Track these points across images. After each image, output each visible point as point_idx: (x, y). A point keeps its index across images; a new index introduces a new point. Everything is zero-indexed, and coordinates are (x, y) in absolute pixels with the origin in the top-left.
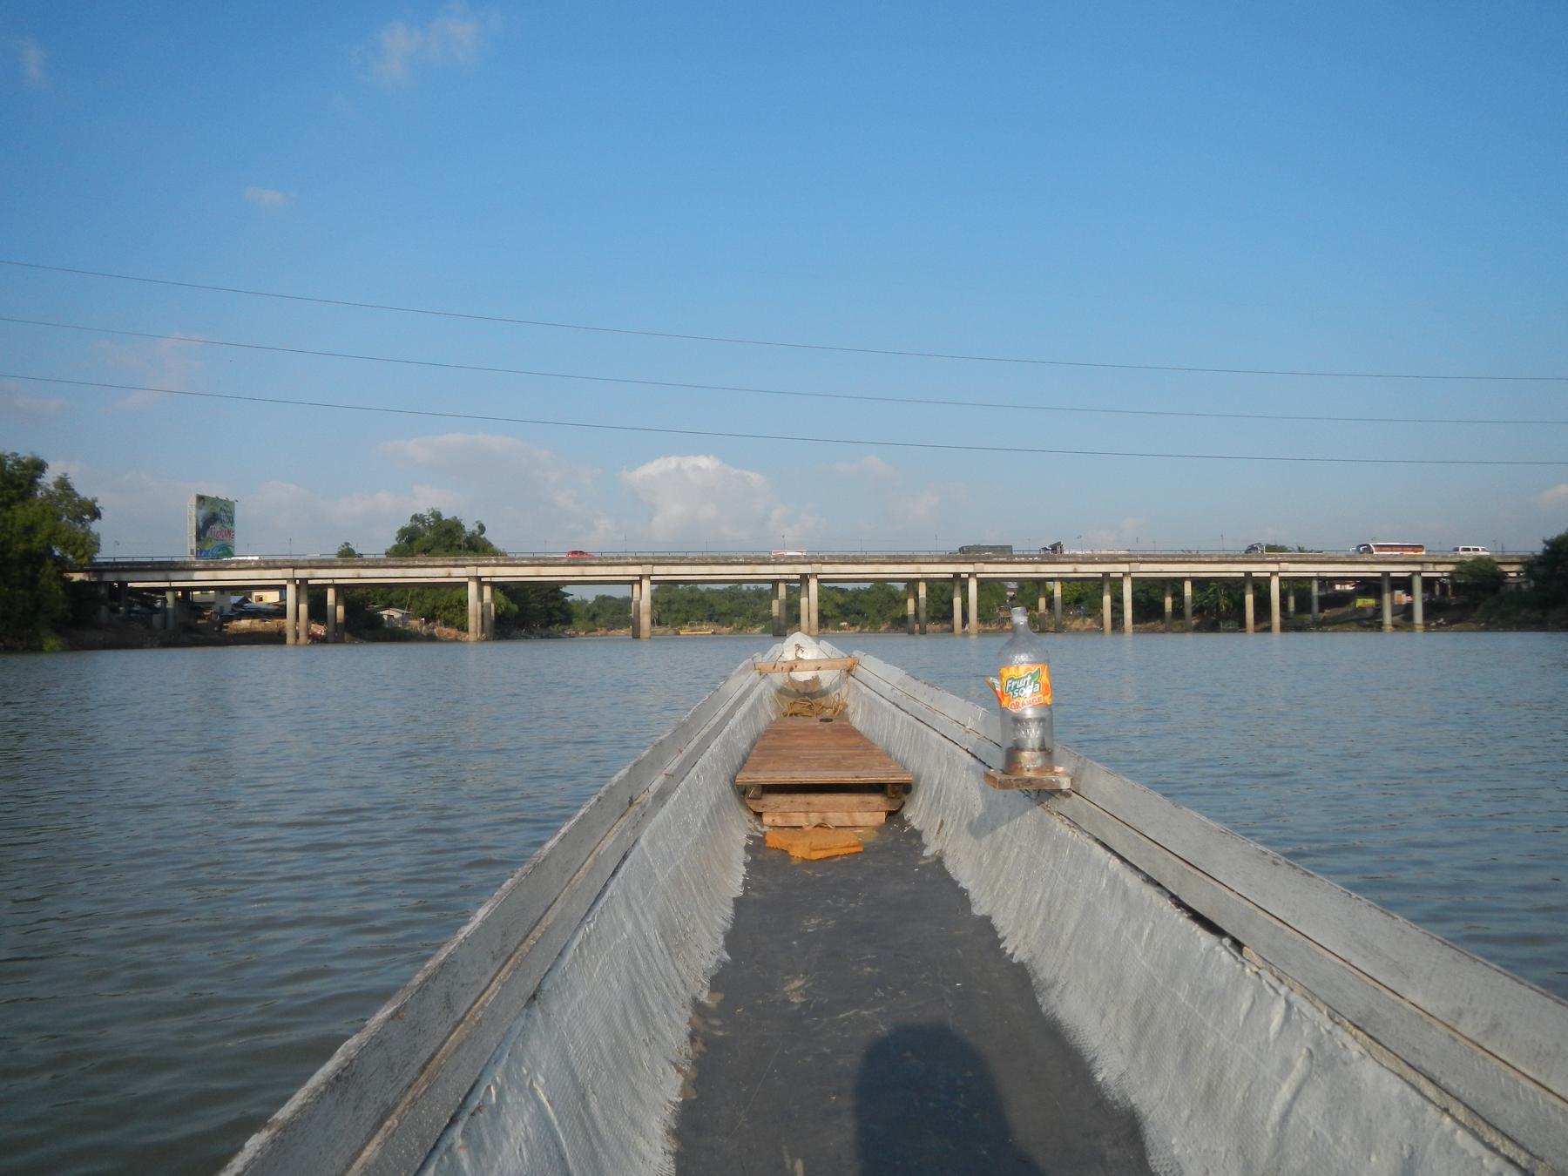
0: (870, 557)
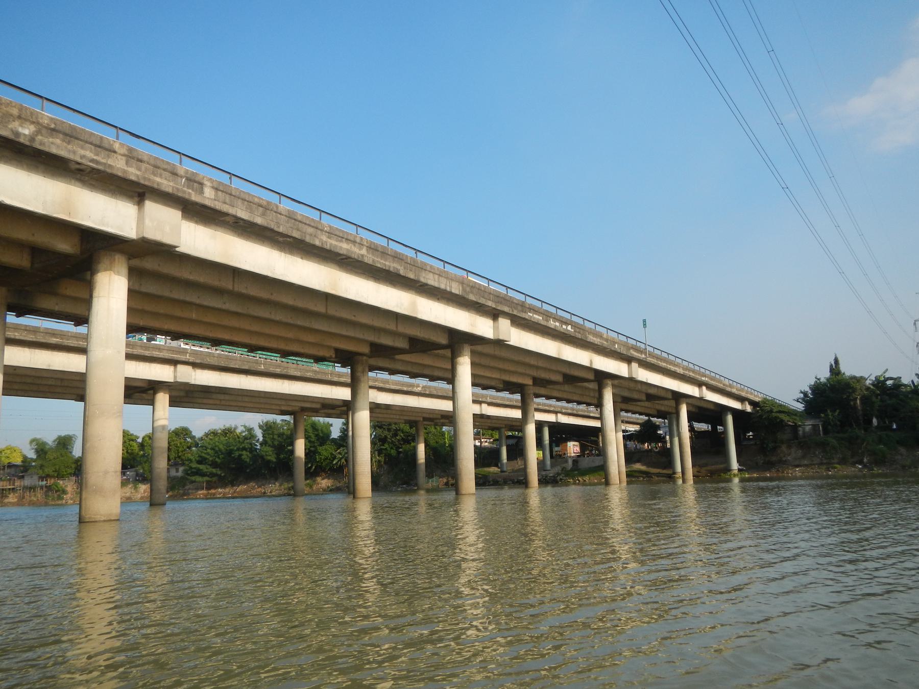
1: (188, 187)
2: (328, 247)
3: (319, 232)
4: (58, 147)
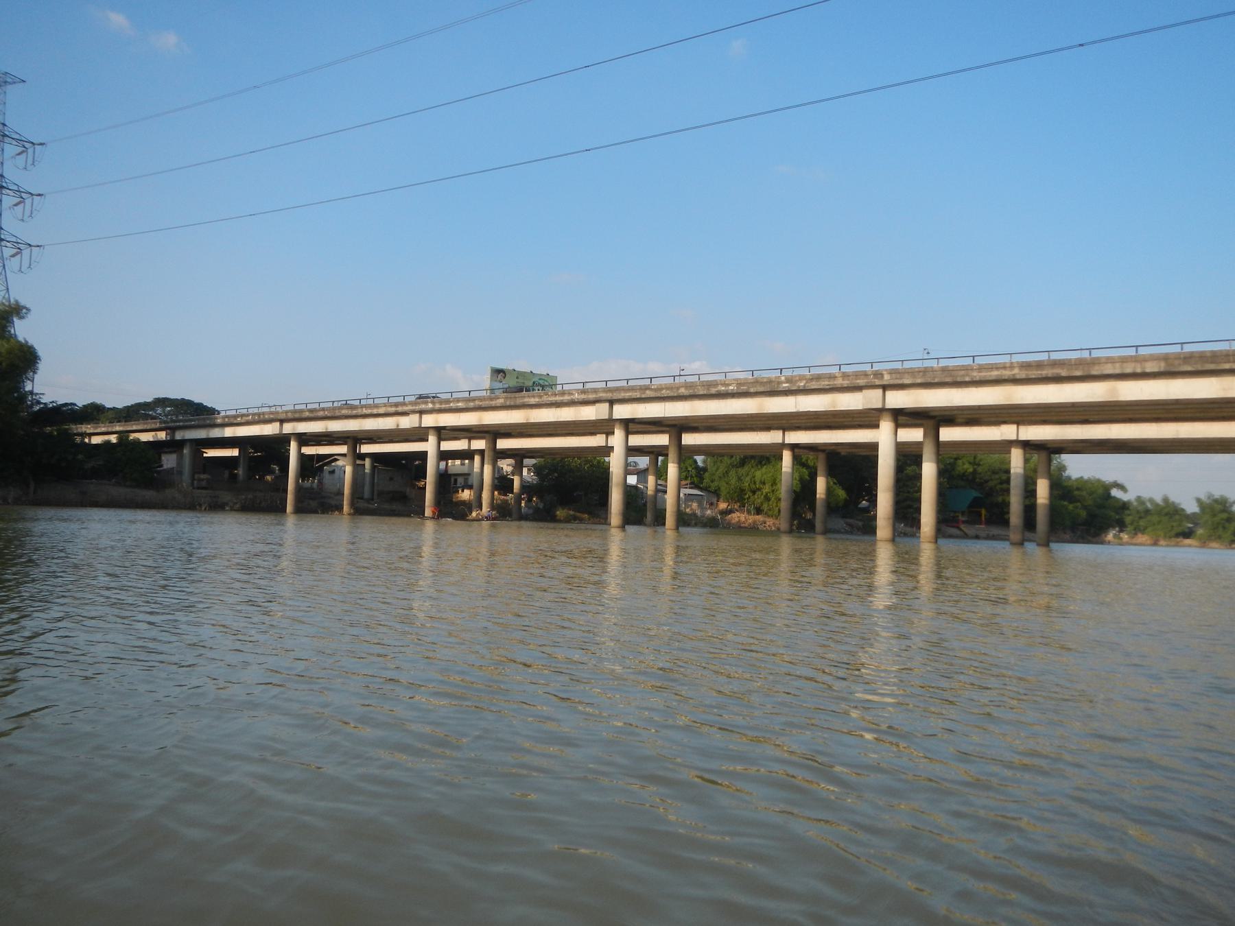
0: (981, 368)
1: (875, 379)
2: (978, 379)
3: (970, 372)
4: (813, 385)
